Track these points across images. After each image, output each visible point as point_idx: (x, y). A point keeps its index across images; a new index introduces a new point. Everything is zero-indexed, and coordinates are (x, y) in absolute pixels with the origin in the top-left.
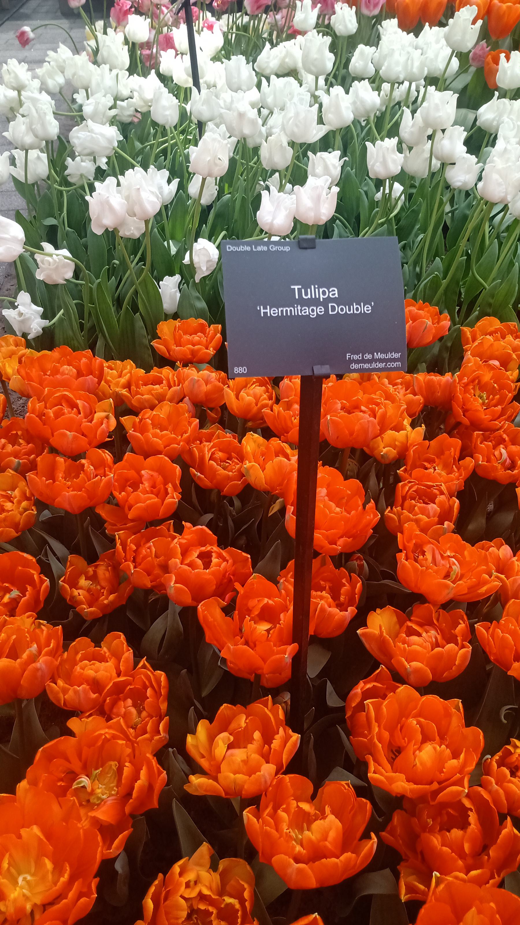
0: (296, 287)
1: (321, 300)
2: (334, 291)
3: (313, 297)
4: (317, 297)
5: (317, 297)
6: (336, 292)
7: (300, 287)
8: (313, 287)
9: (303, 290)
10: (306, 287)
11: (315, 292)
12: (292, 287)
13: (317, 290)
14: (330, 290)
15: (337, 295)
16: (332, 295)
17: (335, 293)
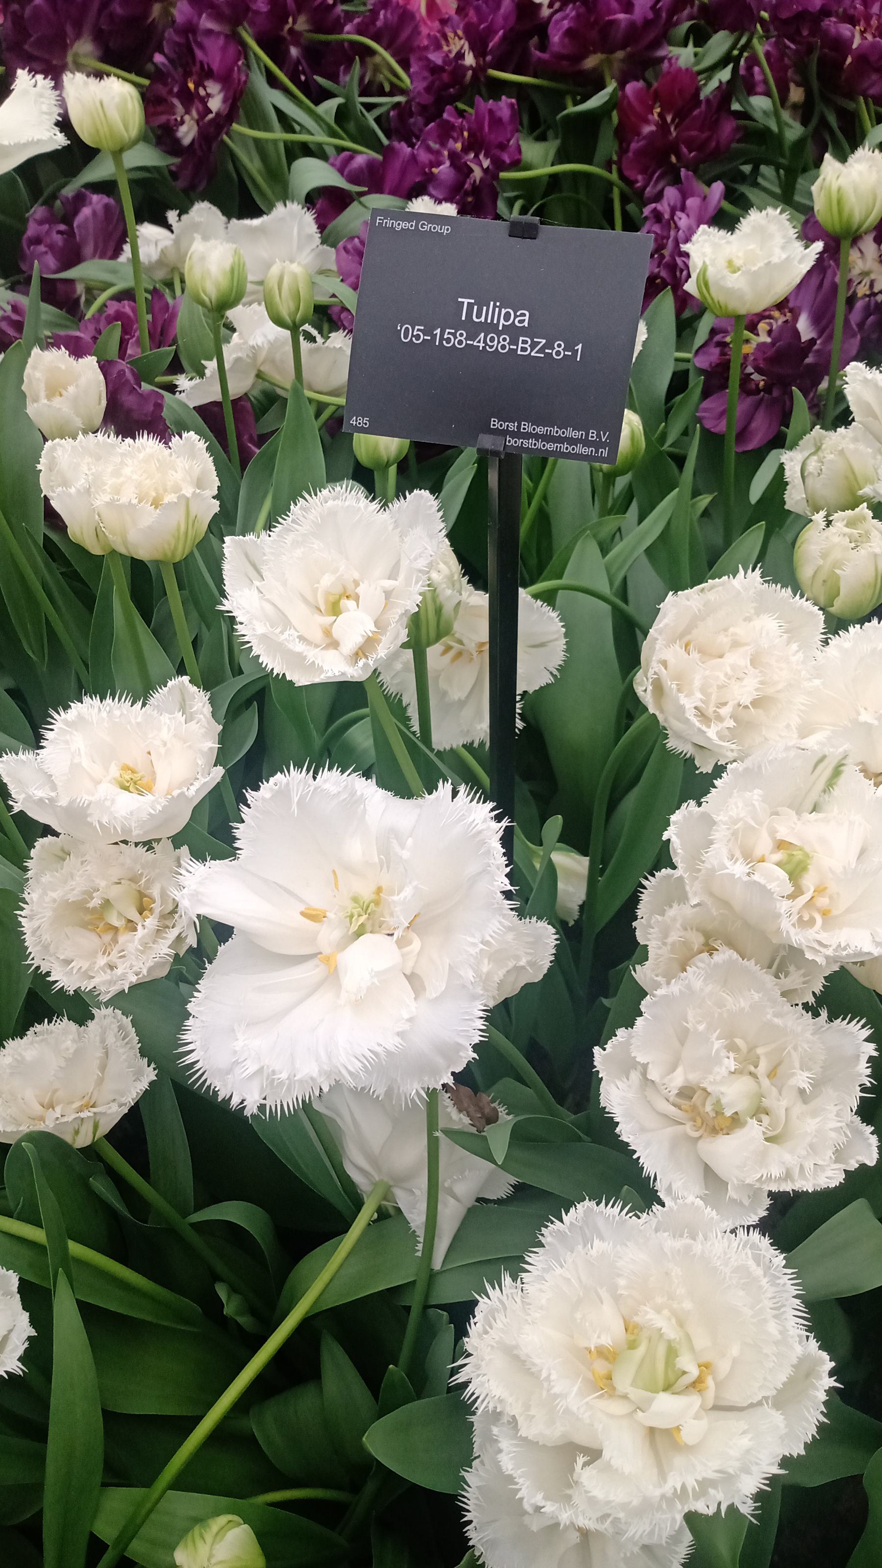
0: (466, 301)
1: (500, 328)
2: (524, 315)
3: (489, 321)
4: (495, 322)
5: (495, 322)
6: (527, 318)
7: (473, 301)
8: (492, 303)
9: (476, 307)
11: (493, 313)
12: (460, 300)
13: (497, 309)
14: (518, 314)
15: (526, 324)
16: (521, 322)
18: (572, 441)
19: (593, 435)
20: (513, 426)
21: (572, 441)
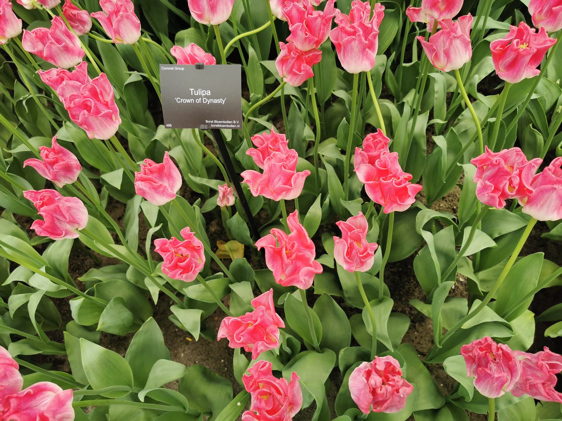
0: (192, 89)
10: (196, 89)
11: (200, 92)
17: (209, 93)
18: (229, 124)
19: (234, 122)
20: (212, 122)
21: (229, 124)
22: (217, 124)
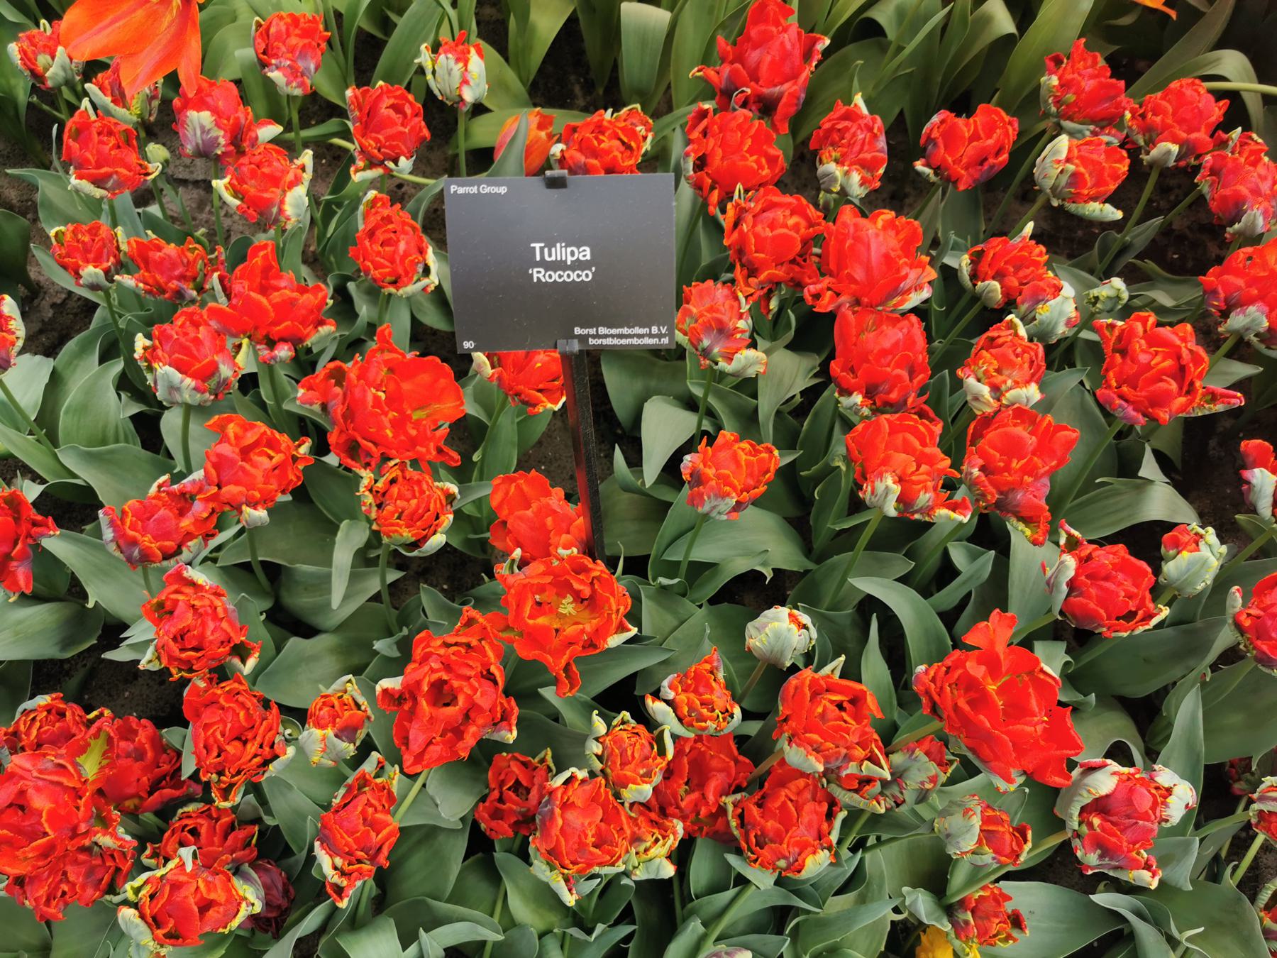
0: (537, 246)
9: (546, 250)
10: (550, 245)
11: (561, 252)
15: (588, 257)
18: (640, 336)
21: (640, 336)
22: (605, 336)
